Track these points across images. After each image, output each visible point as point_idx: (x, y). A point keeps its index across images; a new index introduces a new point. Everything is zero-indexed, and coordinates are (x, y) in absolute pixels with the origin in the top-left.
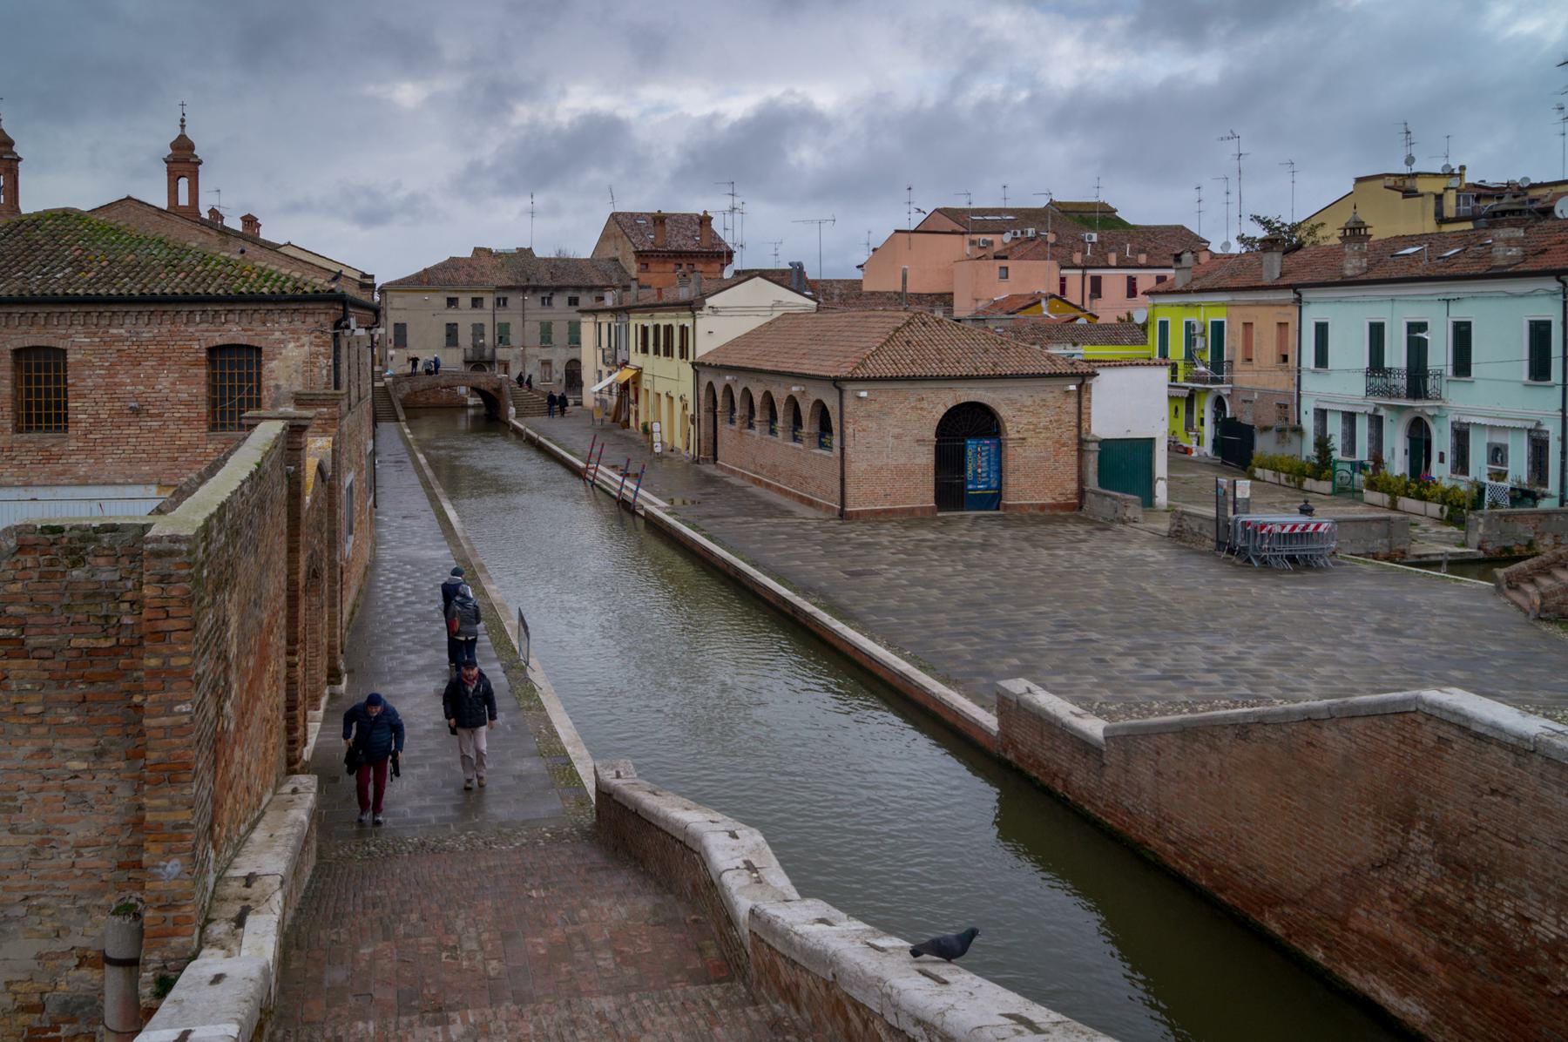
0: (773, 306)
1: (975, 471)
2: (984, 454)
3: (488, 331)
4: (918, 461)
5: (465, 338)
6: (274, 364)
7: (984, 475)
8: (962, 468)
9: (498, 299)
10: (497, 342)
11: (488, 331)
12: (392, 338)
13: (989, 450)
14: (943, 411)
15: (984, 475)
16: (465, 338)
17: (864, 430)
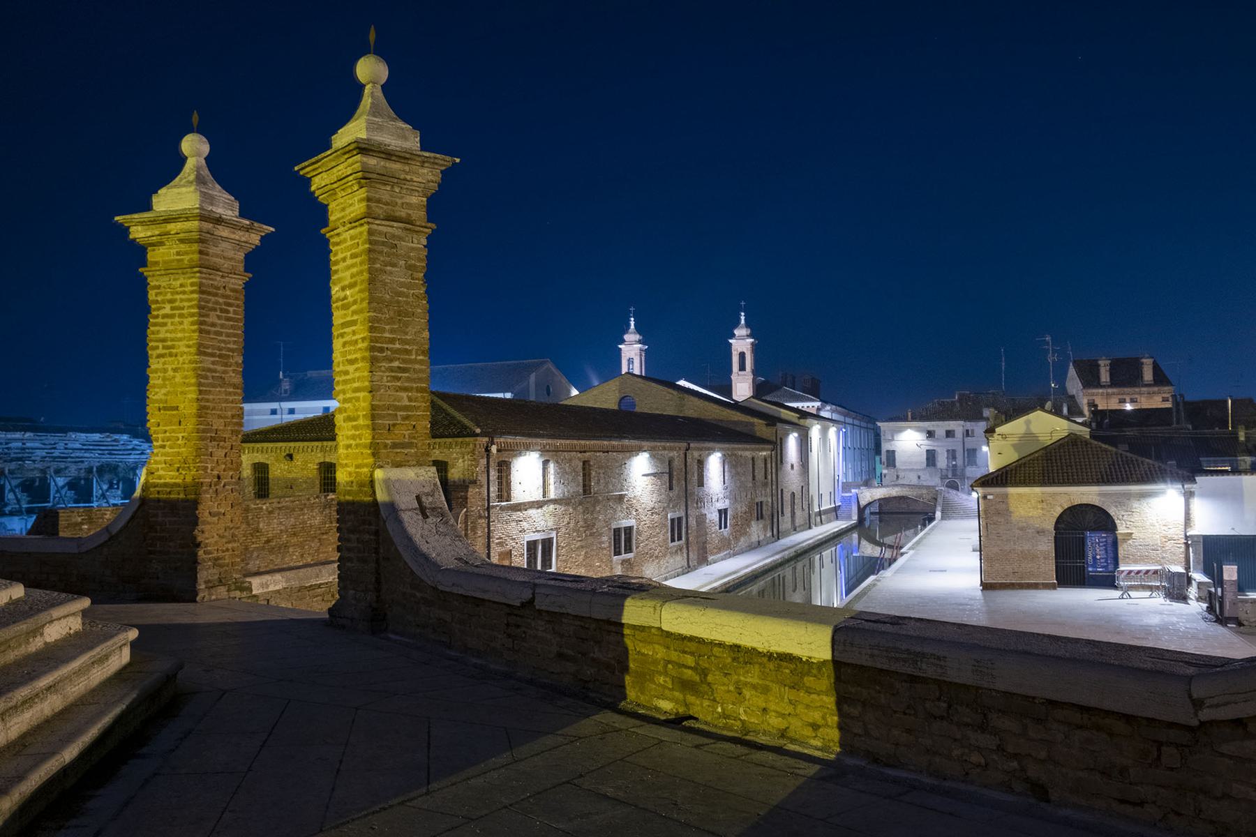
0: (1051, 433)
1: (1094, 558)
2: (1101, 544)
3: (959, 455)
4: (1040, 548)
5: (942, 461)
6: (453, 470)
7: (1102, 561)
8: (1082, 554)
9: (967, 431)
10: (966, 464)
11: (959, 455)
12: (885, 460)
13: (1106, 541)
14: (1059, 510)
15: (1102, 561)
16: (942, 461)
17: (994, 524)
